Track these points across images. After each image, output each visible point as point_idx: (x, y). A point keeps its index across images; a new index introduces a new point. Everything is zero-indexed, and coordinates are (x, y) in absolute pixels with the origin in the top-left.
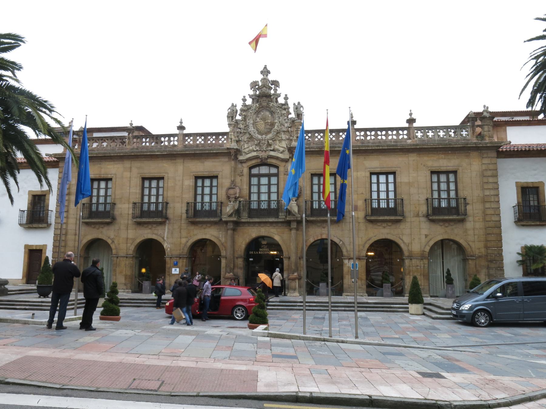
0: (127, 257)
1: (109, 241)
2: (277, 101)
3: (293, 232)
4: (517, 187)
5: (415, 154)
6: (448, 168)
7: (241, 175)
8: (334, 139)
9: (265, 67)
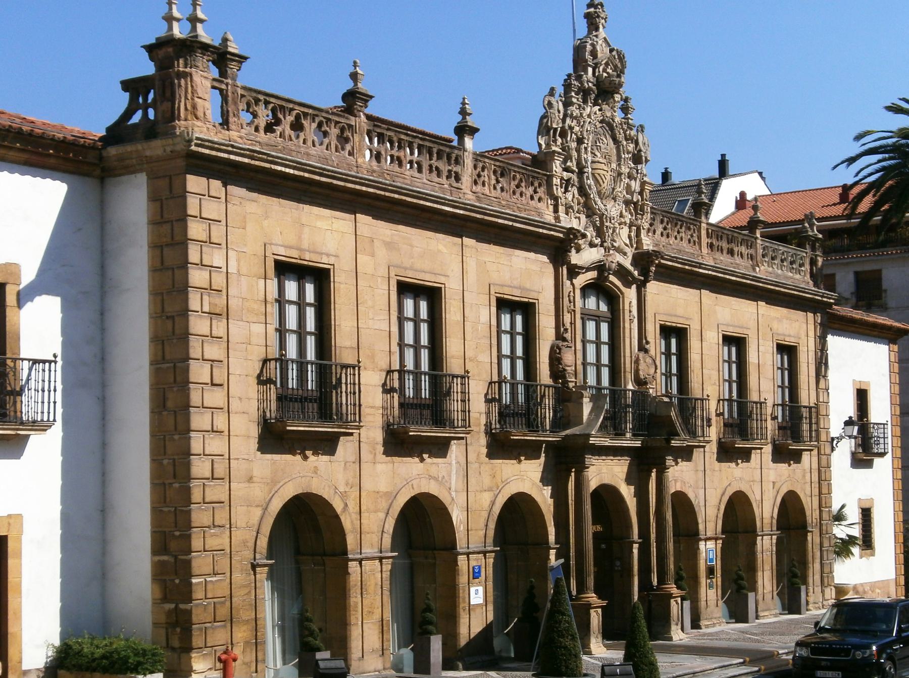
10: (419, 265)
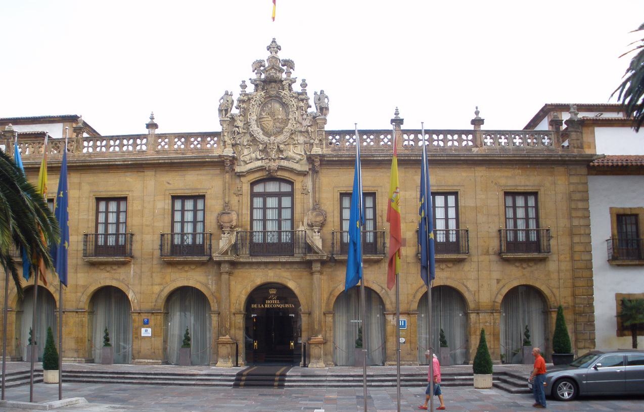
0: (77, 312)
2: (290, 90)
3: (316, 276)
4: (611, 213)
5: (484, 168)
6: (527, 188)
7: (239, 194)
8: (372, 143)
9: (274, 41)
10: (111, 189)
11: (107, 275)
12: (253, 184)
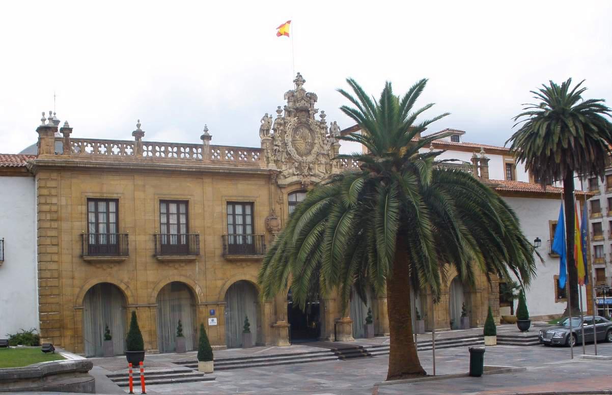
1: (123, 287)
7: (280, 202)
11: (175, 271)
12: (290, 194)
